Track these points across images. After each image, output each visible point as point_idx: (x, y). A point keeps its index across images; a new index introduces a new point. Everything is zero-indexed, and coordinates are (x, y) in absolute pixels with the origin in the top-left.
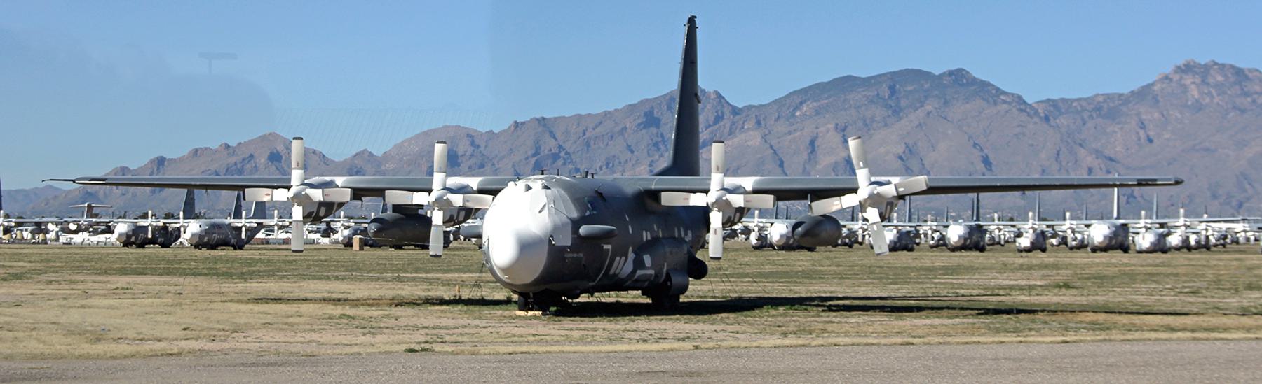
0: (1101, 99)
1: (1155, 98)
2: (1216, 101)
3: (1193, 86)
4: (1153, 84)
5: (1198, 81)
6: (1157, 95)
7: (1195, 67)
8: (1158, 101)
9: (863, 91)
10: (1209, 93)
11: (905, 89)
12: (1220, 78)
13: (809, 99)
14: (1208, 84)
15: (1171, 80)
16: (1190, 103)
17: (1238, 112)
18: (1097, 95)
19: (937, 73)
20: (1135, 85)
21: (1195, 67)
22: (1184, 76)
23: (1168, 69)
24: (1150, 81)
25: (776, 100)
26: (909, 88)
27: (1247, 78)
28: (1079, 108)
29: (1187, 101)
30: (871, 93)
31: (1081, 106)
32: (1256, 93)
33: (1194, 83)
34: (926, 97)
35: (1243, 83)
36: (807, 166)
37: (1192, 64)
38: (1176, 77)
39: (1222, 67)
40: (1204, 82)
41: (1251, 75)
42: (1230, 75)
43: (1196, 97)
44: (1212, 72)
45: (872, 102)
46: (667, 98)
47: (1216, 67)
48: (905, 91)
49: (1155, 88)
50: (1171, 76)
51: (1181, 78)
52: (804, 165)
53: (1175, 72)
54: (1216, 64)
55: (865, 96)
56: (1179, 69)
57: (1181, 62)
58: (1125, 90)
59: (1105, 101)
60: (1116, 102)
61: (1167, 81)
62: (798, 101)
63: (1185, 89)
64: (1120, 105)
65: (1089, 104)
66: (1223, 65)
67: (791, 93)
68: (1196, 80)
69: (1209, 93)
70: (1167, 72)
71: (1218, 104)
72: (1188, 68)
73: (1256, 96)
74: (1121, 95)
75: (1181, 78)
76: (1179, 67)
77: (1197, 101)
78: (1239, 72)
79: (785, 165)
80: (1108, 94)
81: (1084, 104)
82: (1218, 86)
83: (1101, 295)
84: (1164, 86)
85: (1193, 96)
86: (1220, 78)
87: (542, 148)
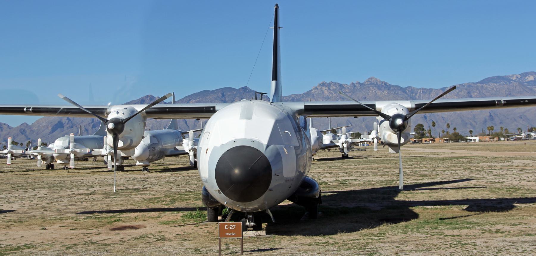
0: (294, 96)
1: (313, 95)
2: (334, 95)
3: (326, 91)
4: (311, 90)
5: (327, 89)
6: (314, 94)
7: (326, 84)
8: (314, 96)
9: (212, 95)
10: (331, 93)
11: (227, 94)
12: (334, 88)
13: (192, 99)
14: (331, 90)
15: (318, 89)
16: (325, 97)
17: (342, 99)
18: (292, 95)
19: (237, 88)
20: (306, 91)
21: (326, 84)
22: (322, 87)
23: (316, 85)
24: (310, 89)
25: (180, 99)
26: (229, 94)
27: (343, 87)
28: (286, 100)
29: (324, 96)
30: (216, 96)
31: (287, 99)
32: (347, 92)
33: (326, 89)
34: (235, 97)
35: (342, 89)
36: (196, 123)
37: (324, 83)
38: (319, 88)
39: (335, 84)
40: (329, 89)
41: (345, 86)
42: (338, 86)
43: (327, 94)
44: (331, 85)
45: (216, 99)
46: (141, 100)
47: (333, 84)
48: (227, 95)
49: (312, 92)
50: (317, 87)
51: (321, 88)
52: (194, 122)
53: (319, 86)
54: (333, 83)
55: (213, 97)
56: (320, 85)
57: (321, 82)
58: (302, 93)
59: (295, 97)
60: (299, 97)
61: (316, 89)
62: (188, 100)
63: (323, 92)
64: (301, 98)
65: (290, 98)
66: (335, 83)
67: (185, 97)
68: (326, 88)
69: (331, 93)
70: (316, 86)
71: (335, 96)
72: (323, 84)
73: (347, 93)
74: (301, 94)
75: (321, 88)
76: (320, 84)
77: (327, 96)
78: (341, 85)
79: (187, 123)
80: (296, 94)
81: (288, 98)
82: (334, 90)
83: (414, 162)
84: (316, 91)
85: (326, 94)
86: (334, 88)
87: (95, 120)
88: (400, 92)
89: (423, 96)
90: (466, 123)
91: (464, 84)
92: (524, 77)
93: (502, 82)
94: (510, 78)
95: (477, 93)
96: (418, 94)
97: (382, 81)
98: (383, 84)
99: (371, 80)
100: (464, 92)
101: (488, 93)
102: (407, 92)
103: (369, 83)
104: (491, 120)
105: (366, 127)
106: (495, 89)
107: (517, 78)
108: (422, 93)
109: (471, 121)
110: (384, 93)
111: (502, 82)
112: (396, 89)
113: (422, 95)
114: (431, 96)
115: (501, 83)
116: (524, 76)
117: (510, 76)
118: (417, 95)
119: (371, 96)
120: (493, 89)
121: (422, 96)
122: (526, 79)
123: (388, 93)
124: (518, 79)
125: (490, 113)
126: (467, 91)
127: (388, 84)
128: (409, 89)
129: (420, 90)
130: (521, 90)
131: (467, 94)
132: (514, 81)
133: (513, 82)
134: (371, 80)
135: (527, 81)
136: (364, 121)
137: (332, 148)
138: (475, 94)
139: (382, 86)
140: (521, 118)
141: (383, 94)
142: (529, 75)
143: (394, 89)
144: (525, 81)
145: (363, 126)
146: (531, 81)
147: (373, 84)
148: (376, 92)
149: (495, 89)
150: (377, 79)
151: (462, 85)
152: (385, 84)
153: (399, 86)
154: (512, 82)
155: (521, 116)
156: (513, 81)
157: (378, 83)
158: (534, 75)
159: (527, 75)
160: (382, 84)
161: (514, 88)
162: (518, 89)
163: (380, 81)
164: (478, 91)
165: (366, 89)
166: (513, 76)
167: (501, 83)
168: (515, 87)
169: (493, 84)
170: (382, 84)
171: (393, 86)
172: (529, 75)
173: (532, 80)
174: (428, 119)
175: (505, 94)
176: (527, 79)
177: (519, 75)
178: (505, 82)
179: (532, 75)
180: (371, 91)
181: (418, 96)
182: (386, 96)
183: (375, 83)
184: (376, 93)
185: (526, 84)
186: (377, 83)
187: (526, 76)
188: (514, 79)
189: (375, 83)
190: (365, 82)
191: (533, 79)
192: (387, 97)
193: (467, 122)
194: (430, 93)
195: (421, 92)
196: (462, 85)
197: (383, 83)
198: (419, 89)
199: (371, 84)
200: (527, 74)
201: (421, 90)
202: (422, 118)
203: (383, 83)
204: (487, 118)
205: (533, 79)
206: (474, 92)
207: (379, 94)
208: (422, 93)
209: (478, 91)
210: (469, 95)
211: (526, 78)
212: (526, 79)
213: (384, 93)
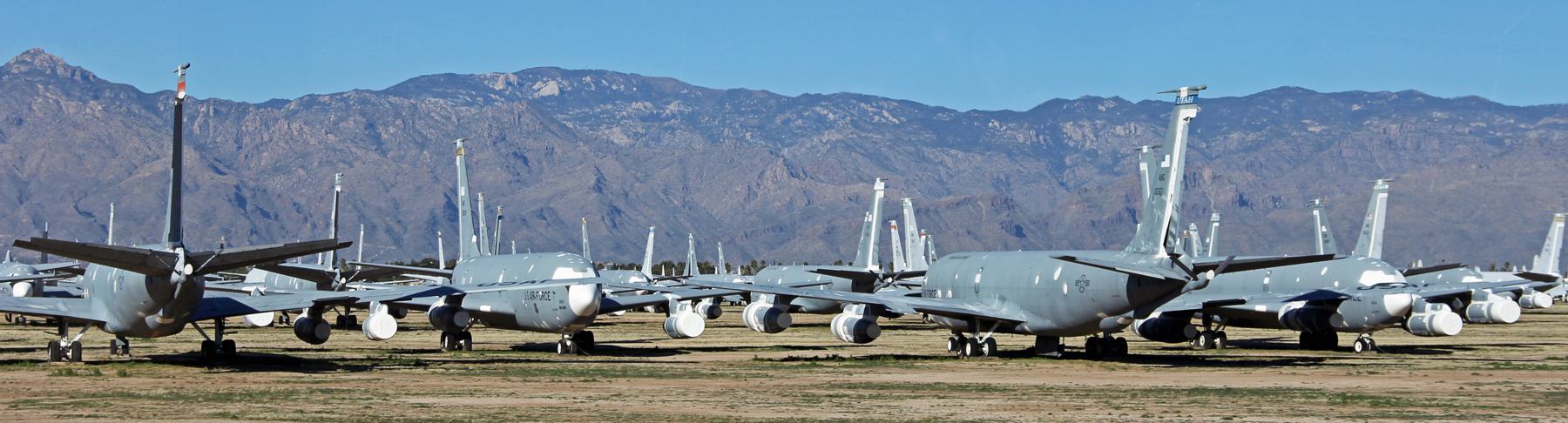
88: (135, 108)
89: (215, 128)
90: (374, 227)
91: (345, 95)
93: (462, 97)
94: (486, 82)
95: (395, 126)
96: (199, 119)
97: (73, 64)
98: (78, 77)
99: (33, 58)
100: (355, 121)
101: (431, 130)
102: (162, 109)
103: (24, 68)
104: (449, 219)
105: (34, 223)
106: (454, 119)
107: (509, 84)
108: (212, 115)
109: (388, 219)
110: (88, 110)
111: (462, 94)
112: (122, 97)
113: (212, 123)
114: (244, 128)
115: (458, 98)
116: (530, 80)
117: (485, 78)
118: (196, 124)
119: (41, 115)
120: (449, 118)
121: (211, 126)
123: (105, 109)
124: (510, 88)
125: (446, 196)
126: (364, 120)
127: (94, 77)
128: (168, 99)
129: (205, 106)
130: (537, 127)
131: (366, 129)
133: (497, 96)
134: (33, 58)
136: (21, 203)
137: (409, 311)
138: (392, 130)
139: (75, 81)
140: (545, 218)
141: (86, 114)
142: (542, 76)
143: (117, 96)
144: (532, 95)
145: (24, 221)
147: (41, 73)
148: (57, 102)
149: (454, 119)
150: (54, 58)
151: (338, 97)
152: (85, 75)
153: (132, 89)
154: (492, 96)
155: (542, 210)
156: (496, 92)
157: (60, 71)
158: (559, 79)
160: (73, 75)
161: (514, 119)
162: (527, 125)
163: (66, 67)
164: (399, 122)
165: (24, 90)
166: (494, 78)
167: (458, 98)
168: (517, 118)
169: (433, 100)
170: (73, 75)
171: (112, 86)
173: (553, 95)
174: (249, 207)
175: (490, 136)
176: (539, 90)
177: (514, 74)
180: (40, 100)
181: (200, 126)
182: (98, 118)
183: (49, 72)
184: (61, 107)
186: (54, 70)
188: (499, 86)
189: (49, 72)
190: (8, 64)
191: (557, 92)
192: (102, 124)
193: (376, 220)
194: (239, 119)
195: (208, 112)
196: (338, 97)
197: (78, 73)
198: (202, 102)
199: (34, 72)
201: (208, 106)
202: (230, 201)
203: (78, 73)
204: (439, 212)
206: (386, 125)
207: (72, 110)
208: (212, 115)
209: (399, 122)
210: (372, 133)
211: (535, 87)
213: (88, 110)
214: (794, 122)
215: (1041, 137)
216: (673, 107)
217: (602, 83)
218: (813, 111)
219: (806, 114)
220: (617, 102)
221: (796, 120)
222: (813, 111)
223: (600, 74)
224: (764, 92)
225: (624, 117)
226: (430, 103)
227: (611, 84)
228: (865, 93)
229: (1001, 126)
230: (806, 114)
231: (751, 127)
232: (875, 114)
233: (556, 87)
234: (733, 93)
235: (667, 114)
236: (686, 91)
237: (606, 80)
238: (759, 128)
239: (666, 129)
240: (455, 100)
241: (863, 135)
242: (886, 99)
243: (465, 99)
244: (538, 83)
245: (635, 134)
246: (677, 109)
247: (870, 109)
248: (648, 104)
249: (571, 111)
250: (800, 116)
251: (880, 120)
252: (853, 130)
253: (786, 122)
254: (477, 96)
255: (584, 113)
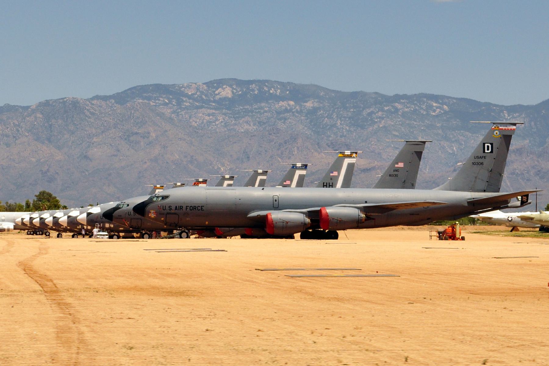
91: (65, 100)
92: (214, 90)
93: (162, 99)
111: (162, 97)
115: (159, 100)
116: (214, 87)
122: (217, 95)
132: (189, 97)
135: (217, 97)
146: (225, 99)
151: (61, 101)
156: (187, 96)
159: (221, 85)
166: (189, 87)
167: (159, 100)
172: (225, 86)
176: (219, 93)
178: (168, 99)
179: (231, 86)
185: (214, 104)
187: (217, 89)
200: (220, 83)
205: (230, 95)
211: (217, 92)
212: (217, 95)
214: (375, 114)
215: (533, 123)
216: (309, 105)
217: (263, 89)
218: (394, 107)
219: (386, 108)
220: (270, 101)
221: (378, 112)
222: (392, 106)
223: (261, 83)
224: (376, 93)
225: (266, 112)
226: (95, 102)
227: (270, 89)
228: (436, 93)
229: (509, 116)
230: (386, 108)
231: (344, 117)
232: (437, 108)
233: (230, 92)
234: (354, 95)
235: (297, 109)
236: (322, 94)
237: (266, 86)
238: (350, 118)
239: (280, 119)
240: (157, 101)
241: (407, 122)
242: (448, 98)
243: (164, 101)
244: (220, 89)
245: (259, 122)
246: (312, 105)
247: (435, 104)
248: (292, 103)
249: (237, 107)
250: (383, 110)
251: (440, 112)
252: (401, 119)
253: (370, 114)
254: (172, 99)
255: (244, 109)
